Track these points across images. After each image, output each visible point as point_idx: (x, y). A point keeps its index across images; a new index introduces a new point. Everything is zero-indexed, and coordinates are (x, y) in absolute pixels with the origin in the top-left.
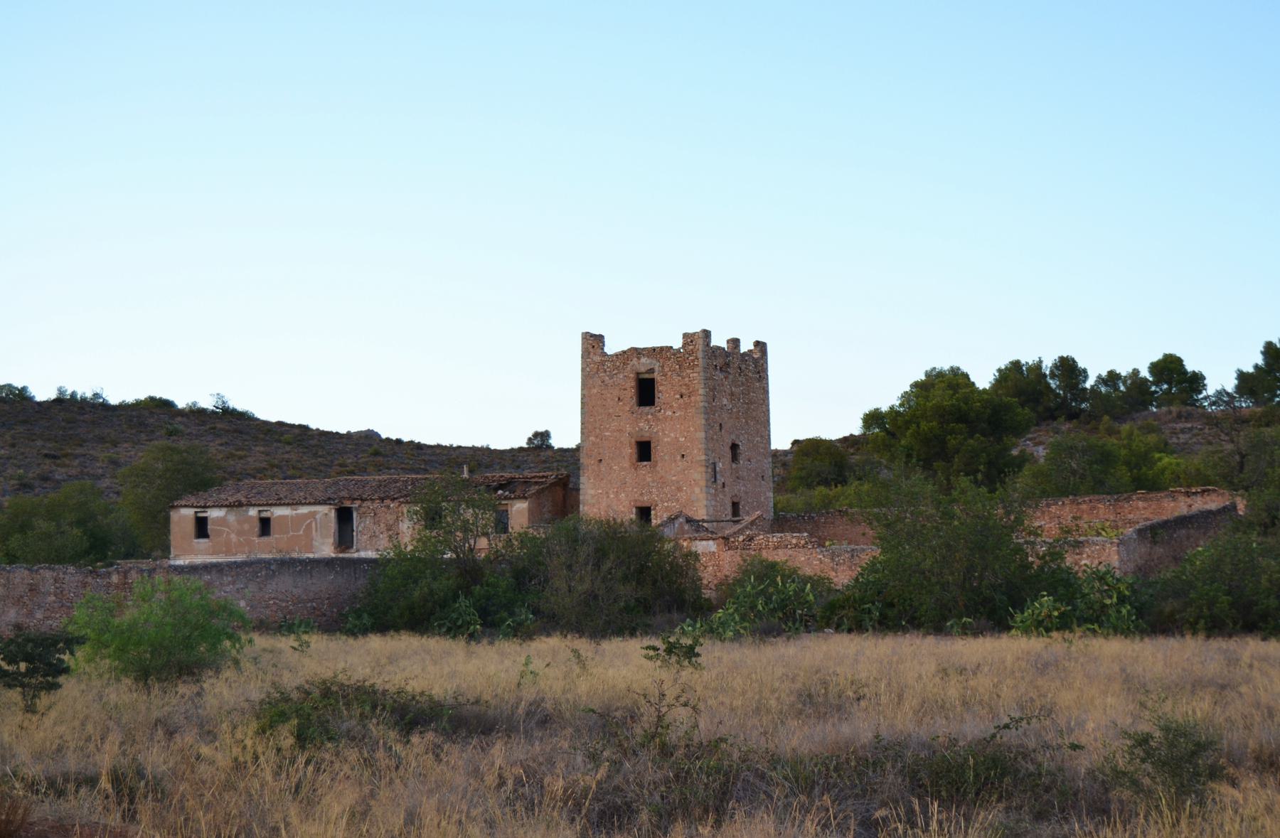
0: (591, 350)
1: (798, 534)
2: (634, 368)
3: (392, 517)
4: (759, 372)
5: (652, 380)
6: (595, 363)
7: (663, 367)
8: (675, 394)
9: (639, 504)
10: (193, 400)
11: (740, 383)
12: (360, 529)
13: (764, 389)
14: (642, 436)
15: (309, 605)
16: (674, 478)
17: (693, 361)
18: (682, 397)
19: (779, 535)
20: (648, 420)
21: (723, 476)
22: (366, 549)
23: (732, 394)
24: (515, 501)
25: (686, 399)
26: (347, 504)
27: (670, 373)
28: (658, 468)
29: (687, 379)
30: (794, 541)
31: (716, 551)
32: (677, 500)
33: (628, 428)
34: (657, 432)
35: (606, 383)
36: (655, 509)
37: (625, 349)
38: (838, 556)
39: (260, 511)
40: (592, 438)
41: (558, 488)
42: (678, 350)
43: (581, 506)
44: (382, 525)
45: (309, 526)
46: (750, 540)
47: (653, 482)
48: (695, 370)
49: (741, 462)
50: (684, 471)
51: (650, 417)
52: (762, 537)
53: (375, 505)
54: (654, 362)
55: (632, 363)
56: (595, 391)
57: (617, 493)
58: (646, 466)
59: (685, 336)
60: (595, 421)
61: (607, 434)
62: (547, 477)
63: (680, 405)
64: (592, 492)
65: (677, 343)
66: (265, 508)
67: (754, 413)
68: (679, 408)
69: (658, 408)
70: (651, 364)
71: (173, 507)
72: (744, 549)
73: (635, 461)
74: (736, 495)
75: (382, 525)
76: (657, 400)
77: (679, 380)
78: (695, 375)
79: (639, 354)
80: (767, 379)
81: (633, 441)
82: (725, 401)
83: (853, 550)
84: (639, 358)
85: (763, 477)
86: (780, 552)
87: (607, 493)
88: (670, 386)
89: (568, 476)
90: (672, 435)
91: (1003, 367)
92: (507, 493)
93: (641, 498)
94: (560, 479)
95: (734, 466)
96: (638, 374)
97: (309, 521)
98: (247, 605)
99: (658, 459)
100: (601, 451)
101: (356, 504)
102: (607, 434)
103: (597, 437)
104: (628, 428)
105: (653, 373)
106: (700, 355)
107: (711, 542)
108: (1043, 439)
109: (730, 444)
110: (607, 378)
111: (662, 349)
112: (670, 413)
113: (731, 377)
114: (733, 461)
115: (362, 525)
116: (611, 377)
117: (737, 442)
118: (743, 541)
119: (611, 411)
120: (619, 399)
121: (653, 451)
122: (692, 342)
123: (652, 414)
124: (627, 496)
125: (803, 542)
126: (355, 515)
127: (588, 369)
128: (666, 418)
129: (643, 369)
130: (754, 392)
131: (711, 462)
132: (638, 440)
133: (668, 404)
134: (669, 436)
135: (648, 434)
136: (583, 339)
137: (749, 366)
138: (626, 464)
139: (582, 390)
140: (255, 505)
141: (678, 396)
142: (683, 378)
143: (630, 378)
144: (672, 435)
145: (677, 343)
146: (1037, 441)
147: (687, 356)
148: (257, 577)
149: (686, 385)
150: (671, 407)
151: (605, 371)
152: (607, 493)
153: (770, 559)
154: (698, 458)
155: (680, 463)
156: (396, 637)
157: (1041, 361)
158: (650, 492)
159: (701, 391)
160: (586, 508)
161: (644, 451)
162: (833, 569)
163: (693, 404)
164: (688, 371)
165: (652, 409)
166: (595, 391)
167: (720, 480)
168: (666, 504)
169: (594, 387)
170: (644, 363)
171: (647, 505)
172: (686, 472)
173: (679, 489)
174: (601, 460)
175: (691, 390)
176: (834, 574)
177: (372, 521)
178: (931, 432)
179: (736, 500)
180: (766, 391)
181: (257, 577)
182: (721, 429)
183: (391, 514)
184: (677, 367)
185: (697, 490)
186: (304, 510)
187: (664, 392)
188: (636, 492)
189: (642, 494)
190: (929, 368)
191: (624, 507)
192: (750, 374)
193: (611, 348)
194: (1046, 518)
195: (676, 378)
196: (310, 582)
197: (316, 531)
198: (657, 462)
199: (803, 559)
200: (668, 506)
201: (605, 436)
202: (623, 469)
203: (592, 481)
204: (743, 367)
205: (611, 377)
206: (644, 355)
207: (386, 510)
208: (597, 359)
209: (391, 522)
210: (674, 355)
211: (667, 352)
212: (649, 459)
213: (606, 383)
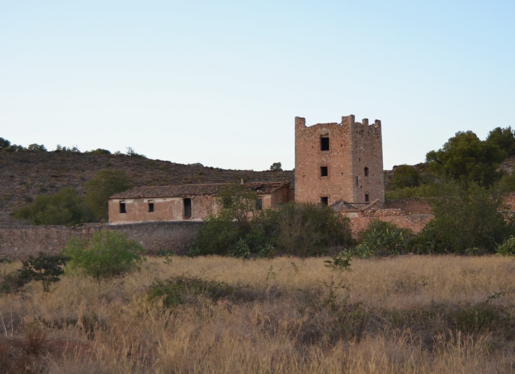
0: (299, 125)
1: (396, 209)
3: (209, 202)
4: (377, 134)
6: (301, 131)
7: (332, 132)
8: (338, 145)
9: (322, 196)
10: (118, 150)
11: (368, 139)
12: (194, 208)
13: (380, 142)
14: (323, 164)
15: (172, 243)
16: (338, 184)
17: (347, 129)
18: (341, 146)
19: (387, 210)
20: (326, 157)
21: (361, 183)
22: (197, 217)
23: (365, 145)
24: (265, 195)
25: (343, 147)
26: (188, 197)
27: (336, 135)
28: (331, 179)
29: (344, 138)
30: (394, 212)
31: (358, 217)
32: (340, 194)
34: (331, 162)
35: (306, 140)
36: (329, 198)
38: (415, 219)
39: (149, 201)
40: (300, 166)
41: (284, 189)
42: (340, 125)
43: (295, 197)
44: (204, 207)
45: (171, 207)
46: (373, 212)
47: (329, 185)
49: (370, 176)
50: (343, 180)
51: (327, 155)
52: (379, 210)
53: (201, 197)
54: (329, 130)
55: (318, 131)
56: (301, 144)
57: (312, 191)
58: (325, 178)
59: (343, 118)
60: (302, 158)
61: (307, 163)
62: (279, 184)
64: (300, 190)
65: (339, 121)
66: (151, 199)
67: (375, 154)
69: (331, 151)
70: (327, 131)
71: (110, 199)
72: (371, 216)
73: (320, 176)
74: (367, 191)
75: (204, 207)
76: (330, 148)
77: (340, 139)
78: (348, 136)
79: (322, 126)
80: (381, 137)
81: (319, 167)
82: (362, 148)
83: (422, 216)
84: (321, 129)
85: (379, 183)
86: (388, 217)
88: (336, 141)
89: (289, 183)
91: (492, 131)
92: (261, 191)
93: (323, 193)
94: (285, 184)
95: (366, 178)
96: (321, 136)
97: (171, 205)
98: (144, 243)
100: (304, 171)
101: (193, 197)
102: (307, 163)
105: (328, 135)
106: (350, 126)
107: (356, 213)
108: (511, 164)
109: (364, 168)
110: (307, 138)
111: (332, 124)
113: (364, 136)
114: (365, 176)
115: (195, 206)
116: (309, 137)
117: (367, 167)
118: (371, 212)
119: (309, 153)
120: (312, 147)
122: (346, 120)
123: (328, 154)
125: (398, 213)
126: (192, 202)
127: (298, 134)
128: (334, 156)
129: (323, 133)
130: (375, 144)
131: (355, 176)
132: (321, 166)
133: (335, 149)
134: (336, 164)
135: (326, 164)
136: (295, 120)
137: (373, 131)
138: (316, 177)
139: (295, 143)
140: (147, 198)
141: (340, 146)
142: (342, 137)
143: (317, 137)
144: (337, 164)
145: (339, 121)
146: (508, 165)
147: (344, 127)
148: (148, 230)
149: (343, 140)
150: (337, 151)
152: (307, 191)
153: (383, 221)
155: (341, 177)
156: (211, 257)
157: (510, 128)
158: (327, 190)
159: (350, 143)
160: (298, 198)
161: (324, 171)
162: (412, 225)
164: (344, 134)
166: (301, 144)
167: (360, 184)
168: (335, 196)
169: (301, 142)
170: (324, 131)
172: (344, 181)
173: (341, 189)
174: (304, 176)
175: (346, 142)
176: (413, 227)
177: (200, 205)
178: (458, 161)
179: (367, 194)
180: (380, 143)
181: (148, 230)
182: (360, 161)
183: (208, 201)
184: (339, 132)
185: (349, 189)
186: (169, 200)
187: (333, 144)
188: (321, 190)
189: (323, 191)
190: (457, 132)
192: (373, 135)
193: (309, 123)
194: (513, 201)
195: (339, 138)
196: (172, 232)
197: (175, 209)
198: (330, 176)
199: (398, 221)
200: (335, 197)
201: (306, 164)
203: (300, 185)
204: (370, 132)
205: (309, 137)
206: (324, 127)
207: (206, 199)
208: (302, 129)
209: (208, 205)
210: (338, 126)
211: (334, 125)
213: (306, 140)
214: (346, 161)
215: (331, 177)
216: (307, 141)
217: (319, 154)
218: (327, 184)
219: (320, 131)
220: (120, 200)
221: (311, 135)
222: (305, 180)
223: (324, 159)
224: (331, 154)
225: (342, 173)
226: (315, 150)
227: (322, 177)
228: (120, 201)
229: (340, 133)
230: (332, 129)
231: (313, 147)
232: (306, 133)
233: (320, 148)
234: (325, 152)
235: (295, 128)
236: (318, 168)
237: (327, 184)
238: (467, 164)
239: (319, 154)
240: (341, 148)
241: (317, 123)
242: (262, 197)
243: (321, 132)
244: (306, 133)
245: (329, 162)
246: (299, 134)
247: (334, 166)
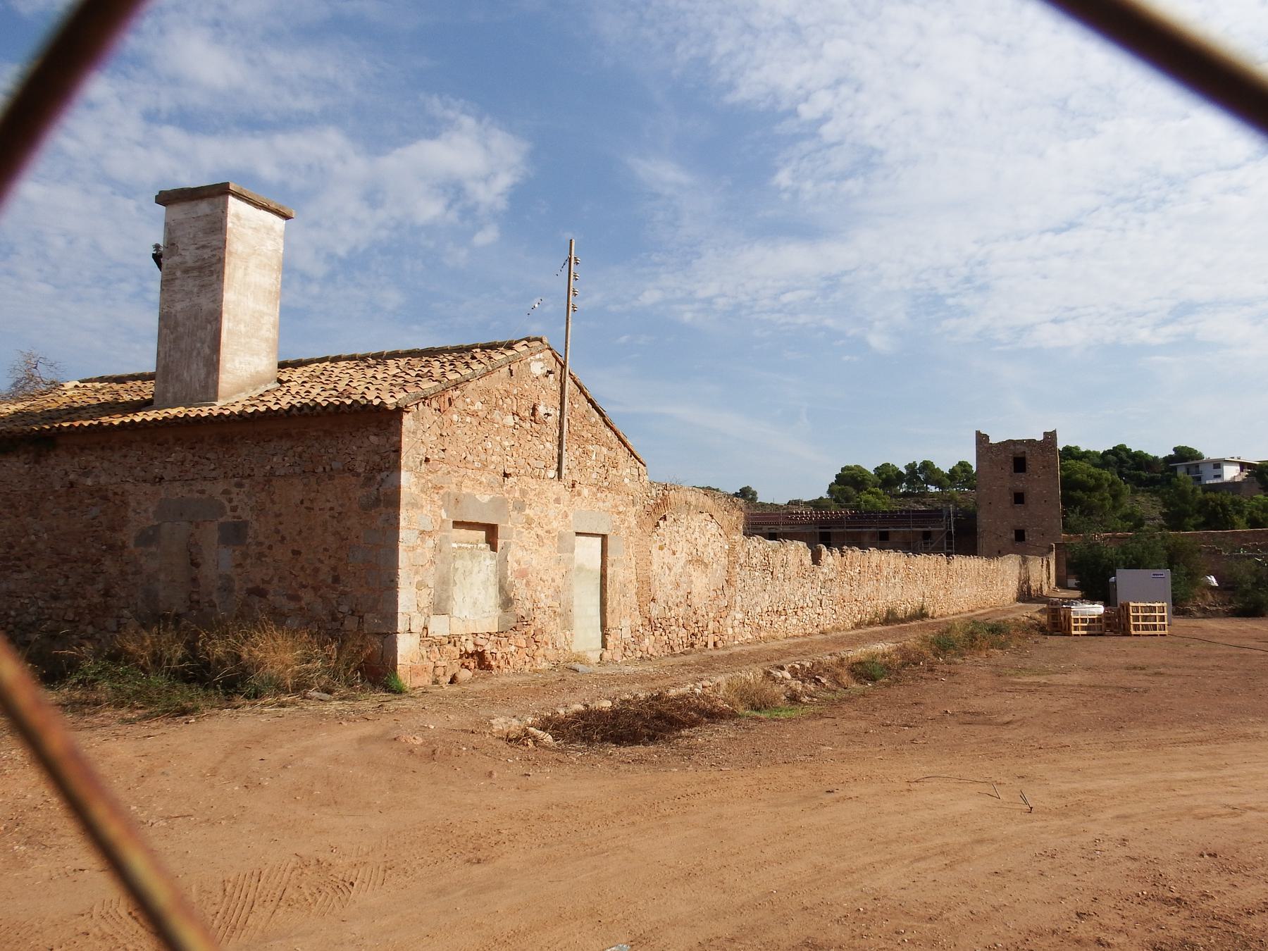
34: (1028, 487)
59: (1045, 433)
65: (1040, 438)
76: (1027, 469)
111: (1029, 441)
150: (1037, 473)
161: (1019, 498)
170: (1021, 448)
171: (1022, 529)
185: (1056, 520)
187: (1031, 464)
212: (1022, 502)
217: (1011, 476)
223: (1021, 483)
239: (1011, 476)
240: (1044, 470)
246: (983, 452)
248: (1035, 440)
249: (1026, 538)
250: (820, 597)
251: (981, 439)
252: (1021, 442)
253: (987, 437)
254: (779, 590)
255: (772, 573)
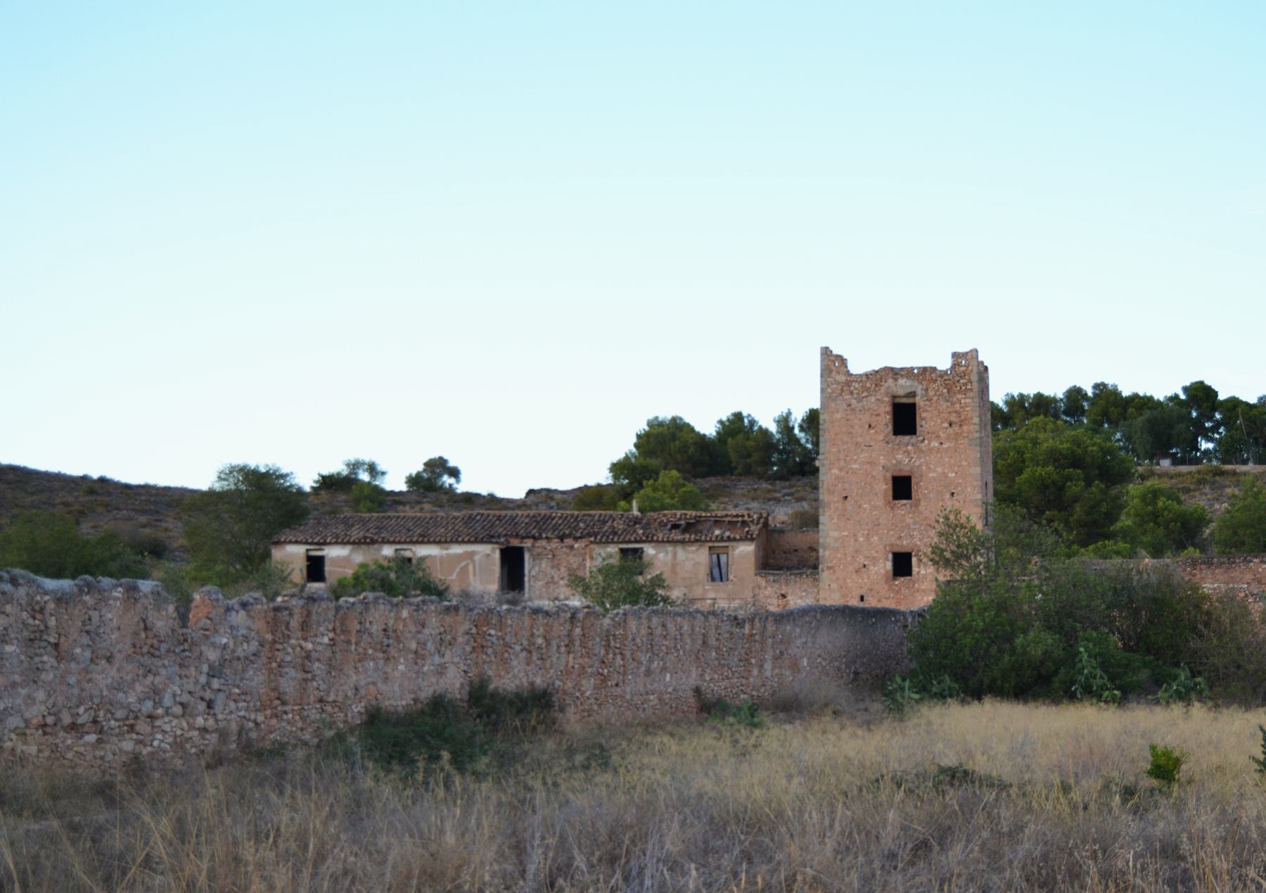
2: (890, 391)
3: (576, 559)
5: (913, 406)
6: (838, 383)
7: (927, 390)
9: (897, 550)
12: (533, 573)
14: (900, 470)
17: (965, 384)
20: (908, 452)
22: (541, 597)
24: (740, 543)
25: (956, 428)
26: (515, 543)
27: (935, 398)
28: (921, 508)
29: (957, 406)
33: (882, 460)
34: (921, 465)
37: (877, 368)
39: (396, 550)
42: (945, 372)
44: (563, 569)
45: (465, 569)
47: (915, 523)
48: (968, 395)
51: (910, 448)
53: (554, 545)
54: (916, 384)
55: (886, 385)
56: (838, 416)
57: (868, 537)
59: (955, 355)
60: (839, 451)
61: (854, 466)
63: (948, 435)
64: (836, 534)
65: (944, 364)
66: (405, 546)
68: (948, 438)
69: (921, 438)
70: (911, 386)
71: (278, 543)
73: (891, 498)
75: (563, 569)
76: (918, 428)
77: (948, 407)
78: (967, 401)
79: (896, 374)
81: (889, 476)
84: (896, 380)
87: (855, 535)
88: (936, 413)
90: (939, 470)
91: (724, 419)
93: (898, 542)
96: (894, 397)
97: (463, 564)
99: (921, 496)
100: (847, 486)
101: (528, 543)
103: (841, 470)
104: (882, 460)
108: (802, 494)
111: (925, 369)
112: (937, 444)
115: (537, 569)
116: (860, 401)
119: (860, 440)
120: (870, 426)
121: (914, 487)
123: (913, 445)
124: (881, 539)
126: (527, 556)
127: (829, 390)
128: (931, 450)
129: (901, 392)
132: (896, 474)
133: (933, 433)
134: (934, 471)
135: (908, 468)
136: (822, 354)
138: (880, 502)
140: (389, 542)
141: (946, 425)
142: (953, 404)
143: (883, 402)
144: (939, 470)
145: (944, 364)
146: (796, 496)
150: (938, 437)
151: (852, 393)
152: (855, 535)
154: (974, 498)
156: (1053, 709)
157: (789, 413)
158: (912, 536)
159: (976, 420)
160: (827, 553)
161: (902, 487)
163: (965, 435)
164: (959, 396)
165: (913, 439)
166: (838, 416)
169: (837, 411)
175: (963, 417)
177: (550, 564)
183: (574, 555)
184: (945, 391)
186: (457, 549)
187: (927, 419)
189: (900, 537)
190: (651, 417)
191: (877, 552)
195: (945, 405)
197: (475, 575)
198: (919, 500)
202: (875, 508)
203: (835, 521)
205: (860, 401)
206: (902, 376)
207: (568, 551)
208: (842, 378)
209: (575, 566)
210: (941, 376)
212: (909, 497)
214: (964, 463)
215: (923, 503)
216: (854, 410)
218: (909, 521)
219: (892, 385)
220: (309, 547)
221: (865, 394)
222: (849, 508)
223: (904, 455)
224: (922, 445)
225: (953, 494)
226: (876, 432)
227: (897, 502)
228: (308, 550)
229: (948, 392)
230: (925, 383)
231: (873, 425)
232: (852, 388)
233: (890, 427)
234: (907, 438)
235: (822, 376)
236: (885, 479)
237: (911, 521)
238: (1069, 483)
239: (887, 443)
240: (950, 430)
241: (882, 366)
242: (730, 549)
243: (894, 389)
244: (852, 388)
245: (917, 464)
247: (931, 475)
248: (934, 369)
249: (915, 569)
250: (208, 695)
251: (832, 363)
252: (908, 372)
253: (843, 361)
254: (79, 682)
255: (56, 646)
